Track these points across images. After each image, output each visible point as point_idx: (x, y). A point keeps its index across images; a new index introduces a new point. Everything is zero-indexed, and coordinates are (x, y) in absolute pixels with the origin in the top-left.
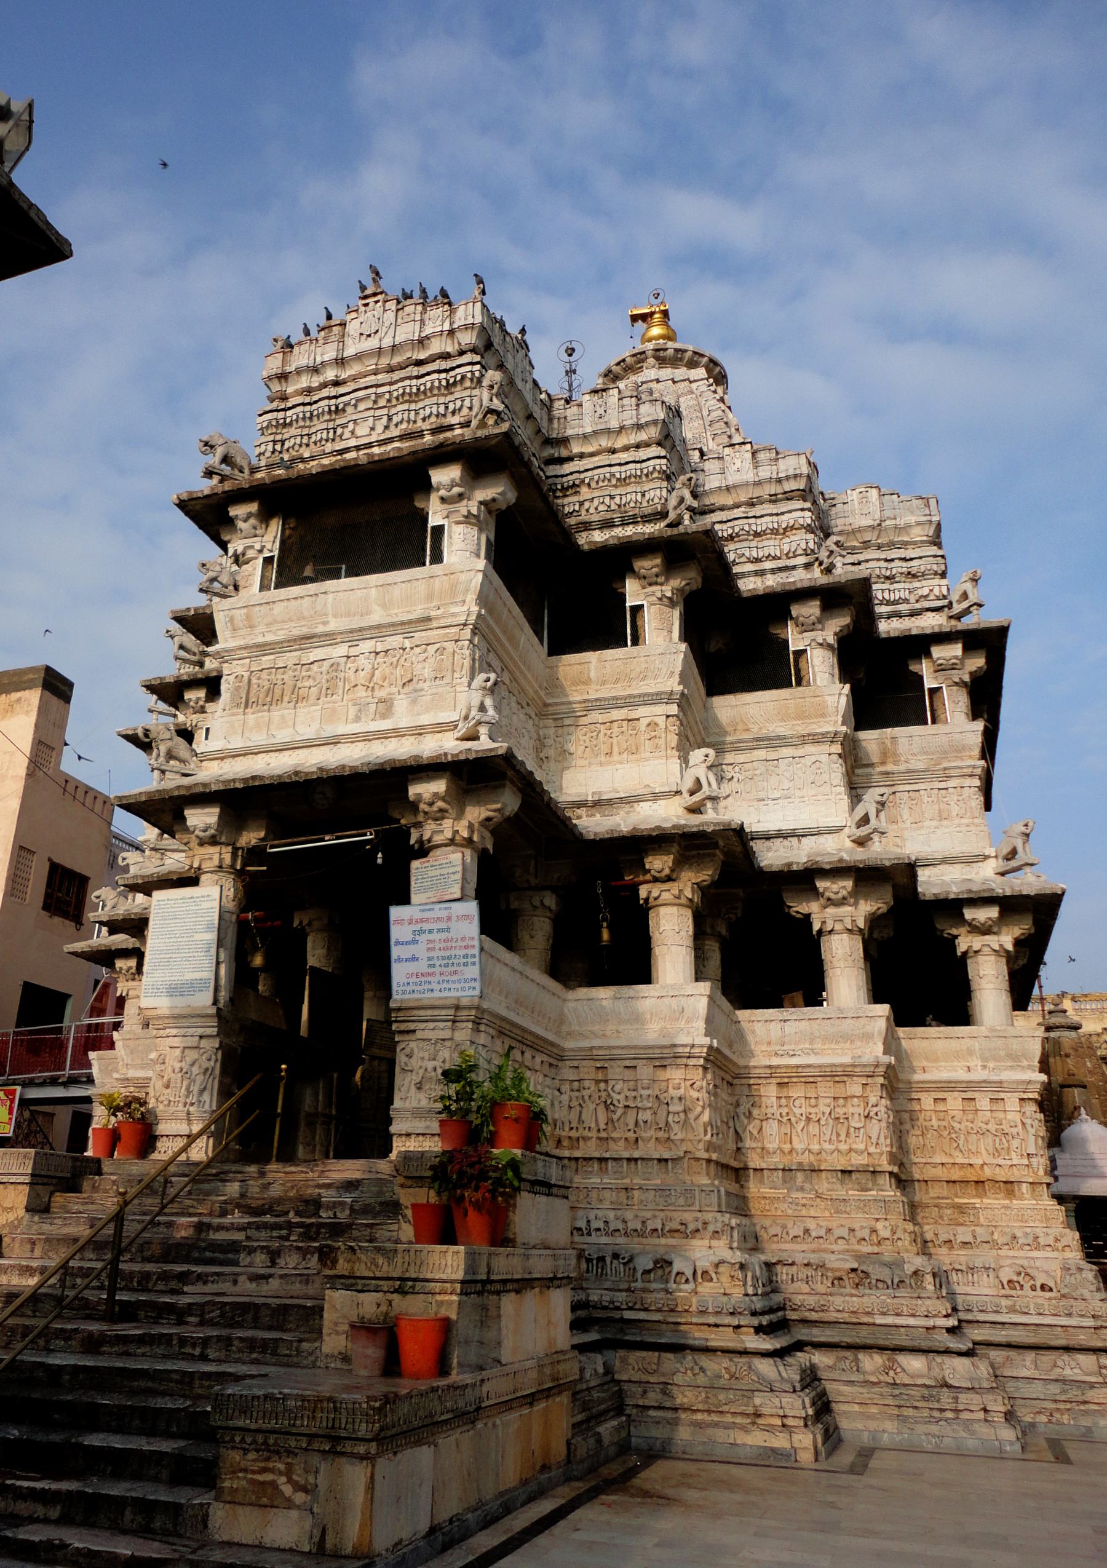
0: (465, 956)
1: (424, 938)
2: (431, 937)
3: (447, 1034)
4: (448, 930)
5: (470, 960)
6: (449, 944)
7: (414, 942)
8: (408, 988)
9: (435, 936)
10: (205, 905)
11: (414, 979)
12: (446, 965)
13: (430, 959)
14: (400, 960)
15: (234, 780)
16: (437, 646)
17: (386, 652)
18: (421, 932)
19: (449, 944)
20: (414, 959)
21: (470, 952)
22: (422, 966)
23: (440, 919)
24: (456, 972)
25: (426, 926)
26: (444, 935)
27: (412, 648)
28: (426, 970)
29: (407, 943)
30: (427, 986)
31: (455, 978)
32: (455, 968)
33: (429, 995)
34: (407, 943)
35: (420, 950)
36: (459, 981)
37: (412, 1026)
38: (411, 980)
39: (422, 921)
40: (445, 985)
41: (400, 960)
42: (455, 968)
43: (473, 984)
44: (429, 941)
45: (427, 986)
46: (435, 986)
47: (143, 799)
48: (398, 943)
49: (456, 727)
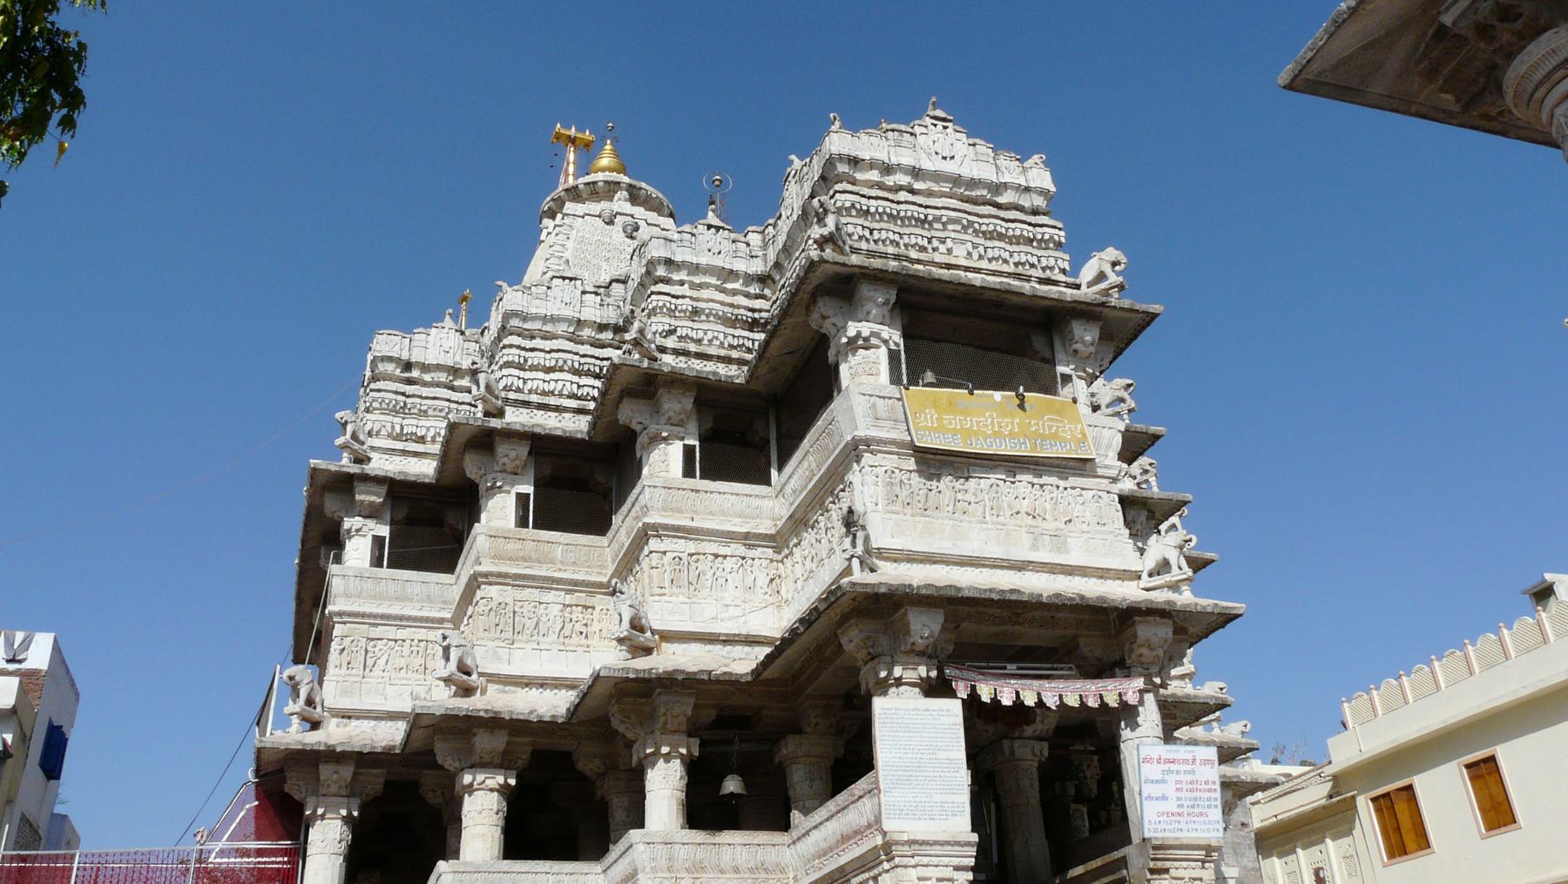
0: (1209, 799)
1: (1172, 778)
2: (1178, 778)
3: (1197, 873)
4: (1193, 772)
7: (1163, 781)
8: (1160, 827)
10: (945, 720)
13: (1179, 799)
14: (1150, 798)
15: (991, 590)
16: (1091, 493)
20: (1164, 798)
21: (1213, 795)
22: (1171, 806)
23: (1186, 761)
24: (1201, 814)
26: (1189, 777)
28: (1176, 810)
31: (1201, 819)
37: (1167, 864)
40: (1192, 826)
41: (1150, 798)
44: (1177, 782)
47: (883, 590)
49: (1139, 578)
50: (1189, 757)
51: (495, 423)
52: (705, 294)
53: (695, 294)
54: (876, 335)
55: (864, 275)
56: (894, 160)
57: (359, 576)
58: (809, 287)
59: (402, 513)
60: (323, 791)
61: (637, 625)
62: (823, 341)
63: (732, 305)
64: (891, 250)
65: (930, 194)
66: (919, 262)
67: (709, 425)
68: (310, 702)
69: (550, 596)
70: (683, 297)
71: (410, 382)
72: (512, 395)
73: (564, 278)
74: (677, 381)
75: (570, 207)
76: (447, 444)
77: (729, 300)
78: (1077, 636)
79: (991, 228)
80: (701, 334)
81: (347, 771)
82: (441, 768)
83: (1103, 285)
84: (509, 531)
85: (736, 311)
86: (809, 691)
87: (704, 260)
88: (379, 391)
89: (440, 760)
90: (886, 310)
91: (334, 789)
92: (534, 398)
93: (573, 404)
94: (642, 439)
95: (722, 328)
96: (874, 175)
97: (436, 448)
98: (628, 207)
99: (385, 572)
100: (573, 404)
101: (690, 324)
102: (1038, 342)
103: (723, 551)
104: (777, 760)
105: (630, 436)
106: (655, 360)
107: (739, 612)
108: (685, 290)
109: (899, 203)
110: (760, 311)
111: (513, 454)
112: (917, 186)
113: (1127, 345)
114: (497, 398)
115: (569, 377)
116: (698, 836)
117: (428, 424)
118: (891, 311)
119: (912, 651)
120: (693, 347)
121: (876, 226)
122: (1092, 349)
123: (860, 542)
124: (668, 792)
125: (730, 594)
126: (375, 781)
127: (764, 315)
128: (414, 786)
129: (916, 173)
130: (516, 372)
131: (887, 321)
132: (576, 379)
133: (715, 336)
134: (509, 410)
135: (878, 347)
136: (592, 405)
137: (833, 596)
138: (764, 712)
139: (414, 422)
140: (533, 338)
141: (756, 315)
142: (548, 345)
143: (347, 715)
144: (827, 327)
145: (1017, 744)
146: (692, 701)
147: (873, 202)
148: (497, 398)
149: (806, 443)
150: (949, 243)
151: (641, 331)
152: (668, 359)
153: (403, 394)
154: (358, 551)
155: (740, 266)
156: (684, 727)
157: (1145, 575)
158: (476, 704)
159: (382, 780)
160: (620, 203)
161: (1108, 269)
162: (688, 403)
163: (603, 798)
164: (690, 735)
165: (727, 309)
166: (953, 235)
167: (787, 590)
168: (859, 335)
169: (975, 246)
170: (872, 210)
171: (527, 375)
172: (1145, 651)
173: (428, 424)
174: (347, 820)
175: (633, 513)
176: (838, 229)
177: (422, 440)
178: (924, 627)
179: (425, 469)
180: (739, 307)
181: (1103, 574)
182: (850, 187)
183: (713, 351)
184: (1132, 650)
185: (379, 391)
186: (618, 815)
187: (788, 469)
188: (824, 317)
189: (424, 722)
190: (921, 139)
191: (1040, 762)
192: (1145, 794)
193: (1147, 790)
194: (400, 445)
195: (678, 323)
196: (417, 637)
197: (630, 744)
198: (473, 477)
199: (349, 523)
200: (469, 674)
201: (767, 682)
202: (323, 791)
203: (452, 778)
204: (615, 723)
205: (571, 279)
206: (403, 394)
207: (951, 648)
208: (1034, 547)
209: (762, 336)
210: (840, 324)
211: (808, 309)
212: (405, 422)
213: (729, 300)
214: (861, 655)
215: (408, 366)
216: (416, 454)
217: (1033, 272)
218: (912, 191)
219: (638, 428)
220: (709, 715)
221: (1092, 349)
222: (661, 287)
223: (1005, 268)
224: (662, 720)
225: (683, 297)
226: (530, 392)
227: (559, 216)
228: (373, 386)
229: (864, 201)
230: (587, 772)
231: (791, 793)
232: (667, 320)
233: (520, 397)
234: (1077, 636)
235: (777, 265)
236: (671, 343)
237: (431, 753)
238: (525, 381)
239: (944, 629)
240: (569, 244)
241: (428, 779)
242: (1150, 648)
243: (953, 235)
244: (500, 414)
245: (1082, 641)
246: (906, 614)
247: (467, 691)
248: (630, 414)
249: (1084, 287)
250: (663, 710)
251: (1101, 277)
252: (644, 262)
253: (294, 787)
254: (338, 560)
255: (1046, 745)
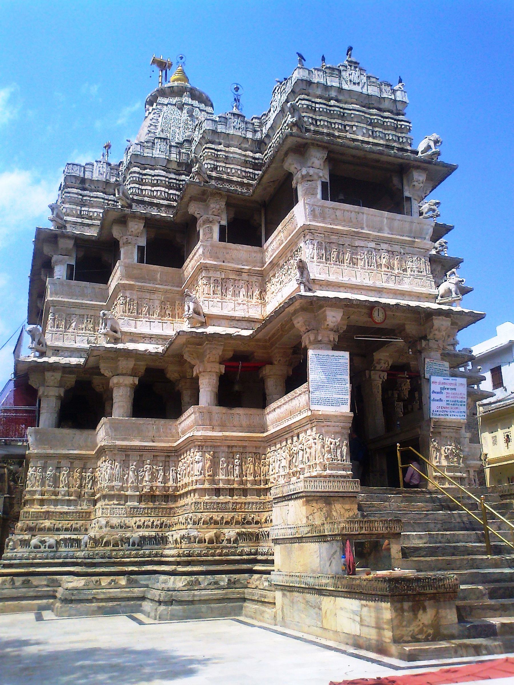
1: (444, 391)
2: (448, 391)
5: (463, 404)
6: (455, 395)
7: (441, 393)
9: (449, 391)
11: (440, 409)
12: (454, 405)
14: (434, 400)
17: (393, 252)
18: (444, 389)
19: (455, 395)
20: (441, 400)
22: (443, 404)
24: (457, 408)
25: (446, 387)
26: (453, 391)
27: (404, 254)
28: (445, 406)
29: (438, 393)
30: (446, 413)
31: (457, 410)
32: (457, 406)
33: (447, 417)
34: (438, 393)
35: (443, 397)
36: (458, 412)
38: (439, 410)
39: (444, 383)
40: (453, 413)
41: (434, 400)
42: (457, 406)
43: (464, 414)
45: (446, 413)
46: (449, 413)
48: (434, 392)
50: (453, 382)
51: (127, 211)
52: (232, 149)
53: (227, 149)
54: (318, 174)
55: (313, 144)
56: (329, 84)
57: (62, 284)
58: (285, 148)
59: (81, 254)
60: (46, 384)
61: (197, 312)
62: (289, 176)
63: (245, 156)
64: (325, 131)
65: (346, 103)
66: (339, 137)
67: (232, 216)
68: (39, 343)
69: (155, 296)
70: (221, 151)
71: (84, 189)
72: (135, 198)
73: (160, 138)
74: (217, 193)
75: (160, 100)
76: (103, 220)
77: (244, 153)
78: (404, 324)
79: (376, 121)
80: (229, 170)
81: (58, 375)
82: (103, 375)
83: (429, 153)
84: (135, 264)
85: (247, 159)
86: (277, 345)
87: (231, 132)
88: (69, 193)
89: (102, 371)
90: (322, 162)
91: (52, 384)
92: (146, 199)
93: (165, 202)
94: (200, 222)
95: (239, 168)
96: (319, 92)
97: (98, 222)
98: (190, 101)
99: (74, 282)
100: (165, 202)
101: (224, 165)
102: (395, 180)
103: (238, 278)
104: (261, 376)
105: (194, 220)
106: (207, 182)
107: (245, 307)
108: (221, 147)
109: (331, 106)
110: (258, 159)
111: (136, 227)
112: (340, 98)
113: (439, 184)
114: (128, 199)
115: (163, 189)
116: (223, 410)
117: (94, 210)
118: (324, 162)
119: (326, 329)
120: (225, 176)
121: (318, 117)
122: (421, 185)
123: (305, 276)
124: (210, 389)
125: (241, 298)
126: (71, 380)
127: (261, 162)
128: (89, 383)
129: (340, 90)
130: (137, 186)
131: (322, 168)
132: (167, 190)
133: (235, 172)
134: (134, 205)
135: (316, 180)
136: (175, 204)
137: (291, 300)
138: (255, 354)
139: (86, 209)
140: (145, 169)
141: (256, 161)
142: (152, 172)
143: (57, 351)
144: (292, 169)
145: (372, 372)
146: (222, 348)
147: (317, 106)
148: (128, 199)
149: (280, 227)
150: (355, 128)
151: (200, 168)
152: (213, 182)
153: (81, 195)
154: (60, 272)
155: (249, 135)
156: (218, 360)
157: (439, 298)
158: (120, 346)
159: (74, 380)
160: (186, 99)
161: (432, 144)
162: (223, 204)
163: (179, 391)
164: (220, 363)
165: (244, 158)
166: (356, 124)
167: (268, 297)
168: (308, 173)
169: (368, 130)
170: (317, 109)
171: (144, 187)
172: (436, 332)
173: (94, 210)
174: (59, 397)
175: (195, 258)
176: (300, 119)
177: (90, 218)
178: (334, 317)
179: (92, 233)
180: (248, 156)
181: (419, 296)
182: (306, 97)
183: (235, 179)
184: (430, 332)
185: (69, 193)
186: (186, 398)
187: (270, 240)
188: (290, 164)
189: (96, 353)
190: (343, 73)
191: (383, 381)
192: (432, 398)
193: (433, 396)
194: (79, 220)
195: (218, 164)
196: (90, 314)
197: (192, 367)
198: (116, 237)
199: (55, 258)
200: (116, 332)
201: (259, 340)
202: (46, 384)
203: (107, 380)
204: (186, 357)
205: (164, 139)
206: (81, 195)
207: (345, 327)
208: (387, 281)
209: (260, 172)
210: (299, 168)
211: (283, 161)
212: (83, 209)
213: (244, 153)
214: (303, 329)
215: (83, 180)
216: (88, 225)
217: (395, 144)
218: (337, 100)
219: (198, 216)
220: (230, 354)
221: (421, 185)
222: (209, 145)
223: (382, 142)
224: (208, 356)
225: (221, 151)
226: (144, 196)
227: (155, 104)
228: (66, 190)
229: (314, 105)
230: (171, 379)
231: (267, 392)
232: (212, 162)
233: (140, 198)
234: (404, 324)
235: (268, 136)
236: (214, 174)
237: (98, 368)
238: (142, 190)
239: (342, 319)
240: (160, 119)
241: (96, 380)
242: (439, 331)
243: (356, 124)
244: (130, 206)
245: (407, 327)
246: (325, 311)
247: (116, 341)
248: (194, 209)
249: (420, 154)
250: (208, 351)
251: (429, 147)
252: (201, 132)
253: (33, 382)
254: (51, 275)
255: (385, 374)
